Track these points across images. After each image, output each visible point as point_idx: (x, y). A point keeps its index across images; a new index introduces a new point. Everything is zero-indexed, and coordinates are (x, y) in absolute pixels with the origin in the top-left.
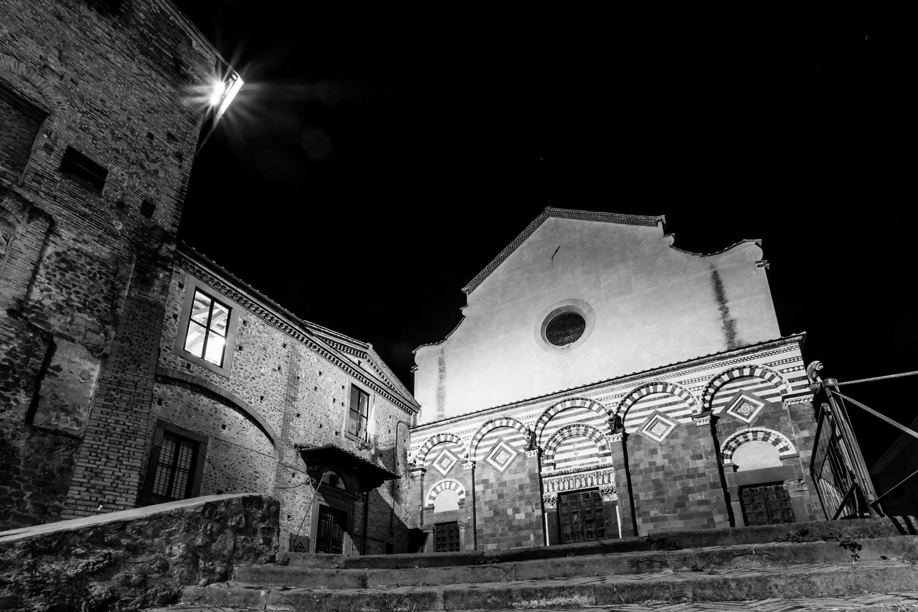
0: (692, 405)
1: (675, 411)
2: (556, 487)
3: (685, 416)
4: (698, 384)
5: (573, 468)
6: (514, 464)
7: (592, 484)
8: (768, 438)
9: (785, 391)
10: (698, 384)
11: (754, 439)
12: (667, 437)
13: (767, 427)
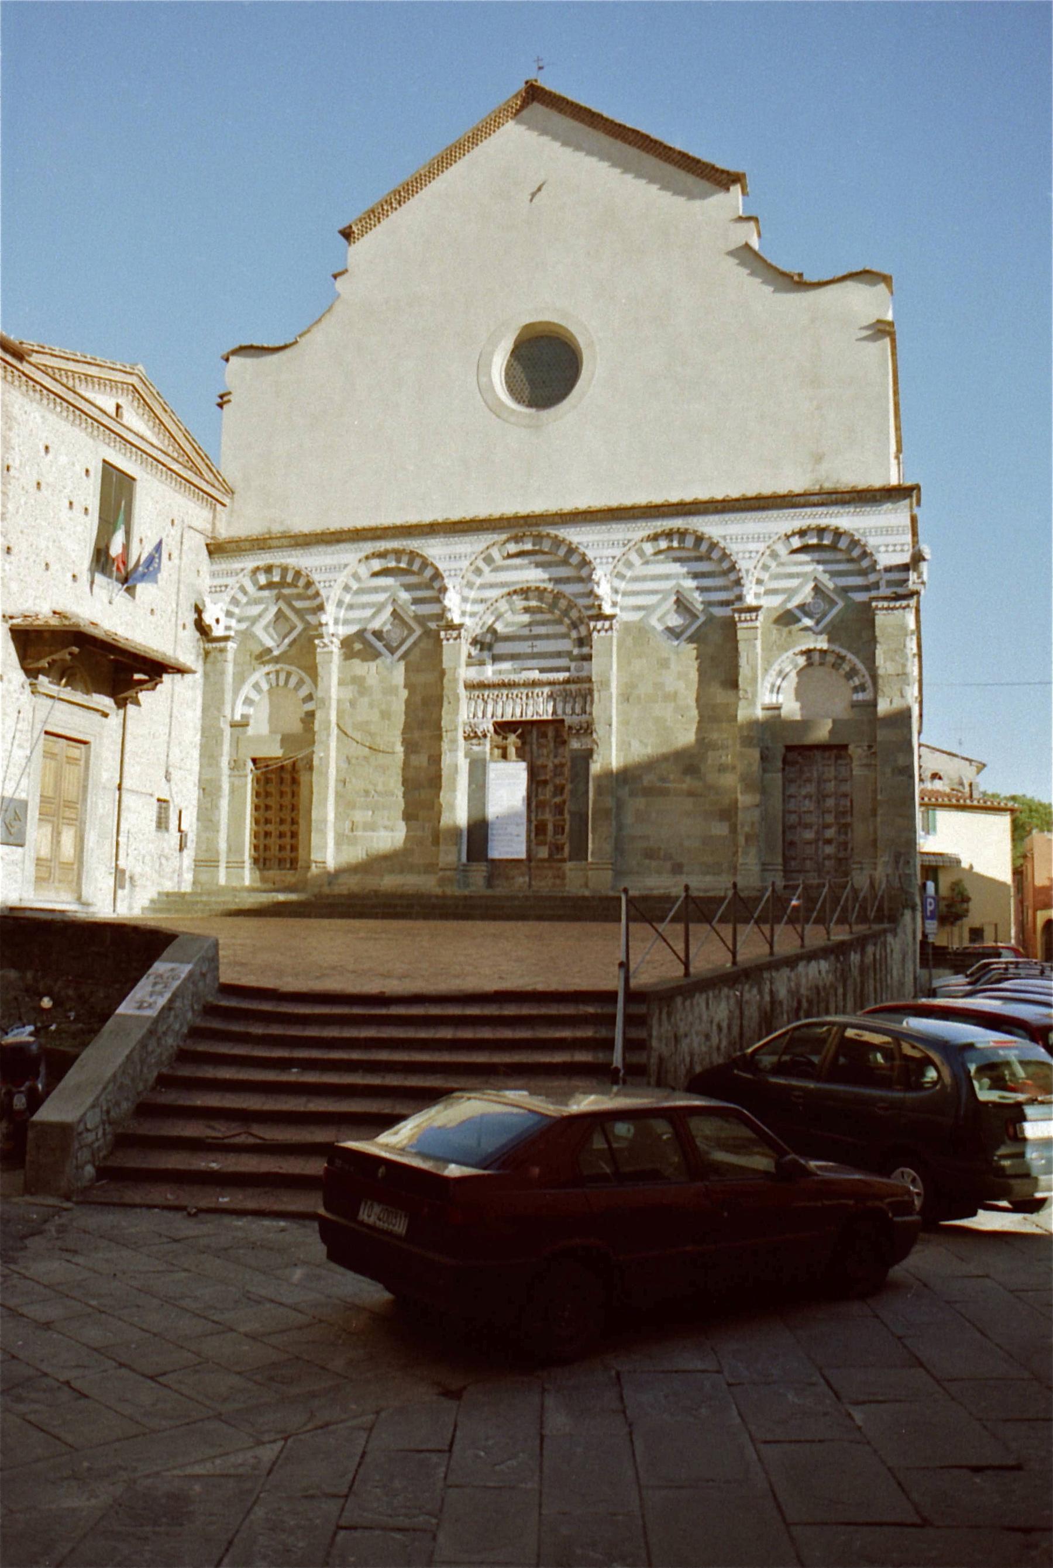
2: (490, 709)
4: (752, 546)
6: (417, 651)
8: (840, 665)
9: (876, 586)
10: (752, 546)
11: (821, 664)
13: (842, 646)
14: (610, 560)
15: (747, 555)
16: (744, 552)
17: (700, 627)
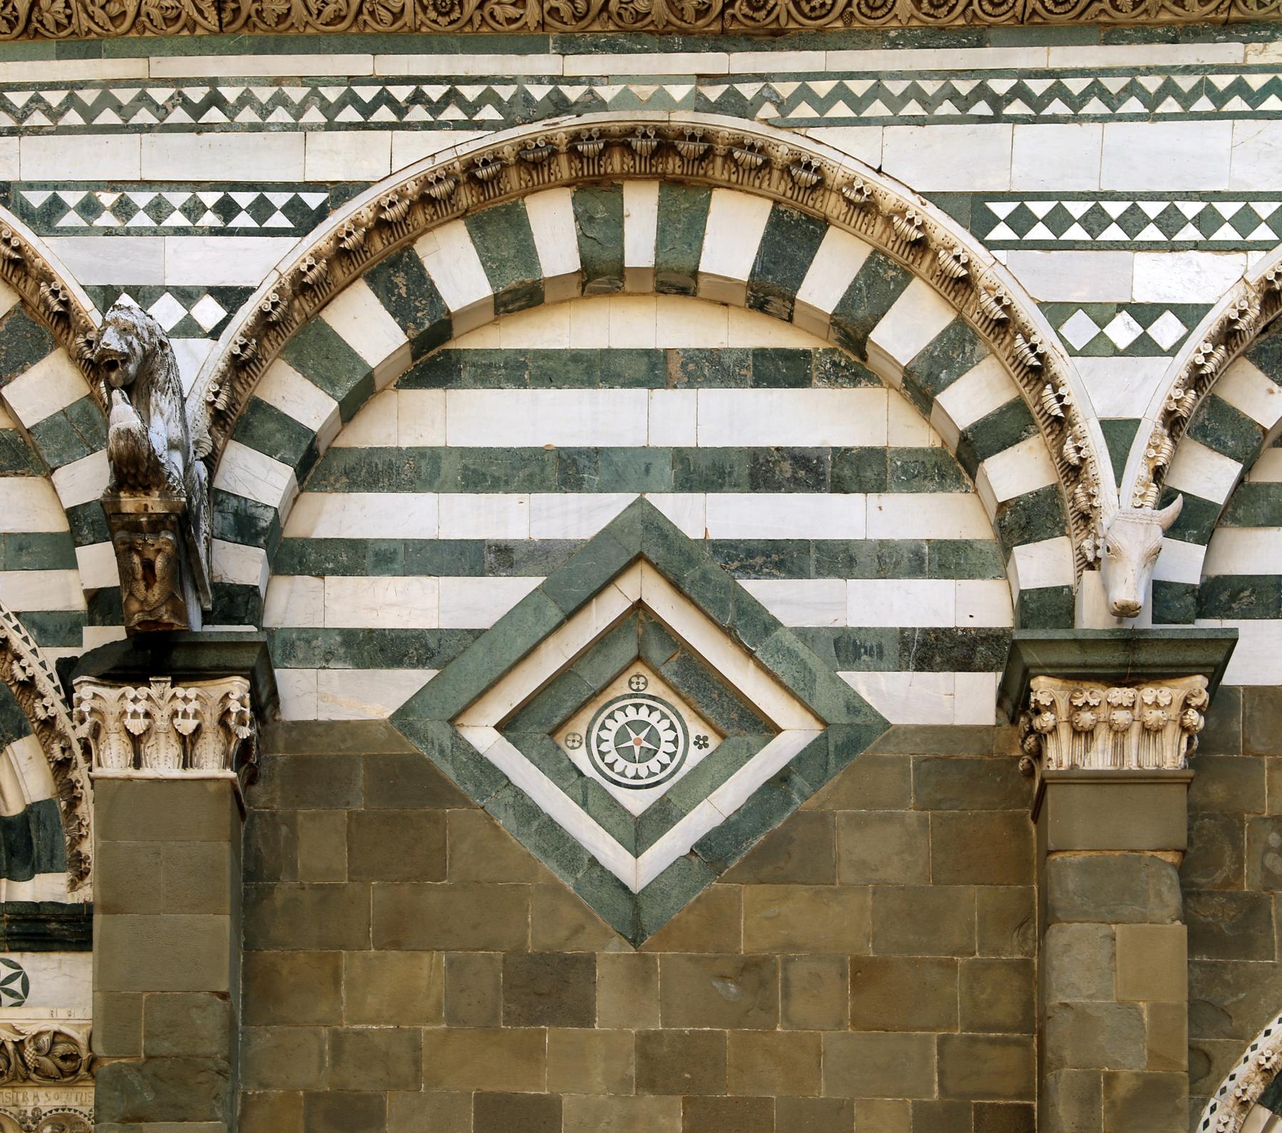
0: (1025, 521)
1: (837, 559)
3: (937, 650)
4: (1155, 276)
10: (1155, 276)
12: (709, 850)
14: (208, 312)
15: (1123, 331)
16: (1102, 314)
17: (782, 778)
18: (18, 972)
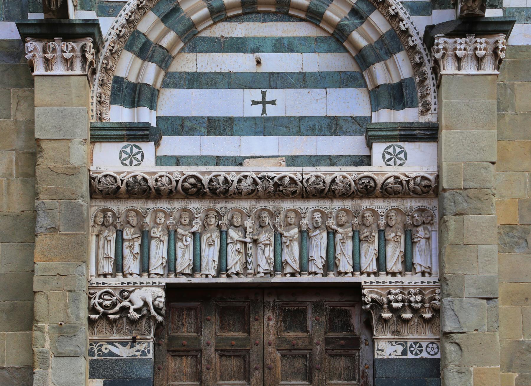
2: (158, 253)
5: (251, 169)
7: (330, 265)
18: (403, 151)
